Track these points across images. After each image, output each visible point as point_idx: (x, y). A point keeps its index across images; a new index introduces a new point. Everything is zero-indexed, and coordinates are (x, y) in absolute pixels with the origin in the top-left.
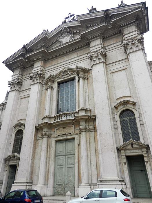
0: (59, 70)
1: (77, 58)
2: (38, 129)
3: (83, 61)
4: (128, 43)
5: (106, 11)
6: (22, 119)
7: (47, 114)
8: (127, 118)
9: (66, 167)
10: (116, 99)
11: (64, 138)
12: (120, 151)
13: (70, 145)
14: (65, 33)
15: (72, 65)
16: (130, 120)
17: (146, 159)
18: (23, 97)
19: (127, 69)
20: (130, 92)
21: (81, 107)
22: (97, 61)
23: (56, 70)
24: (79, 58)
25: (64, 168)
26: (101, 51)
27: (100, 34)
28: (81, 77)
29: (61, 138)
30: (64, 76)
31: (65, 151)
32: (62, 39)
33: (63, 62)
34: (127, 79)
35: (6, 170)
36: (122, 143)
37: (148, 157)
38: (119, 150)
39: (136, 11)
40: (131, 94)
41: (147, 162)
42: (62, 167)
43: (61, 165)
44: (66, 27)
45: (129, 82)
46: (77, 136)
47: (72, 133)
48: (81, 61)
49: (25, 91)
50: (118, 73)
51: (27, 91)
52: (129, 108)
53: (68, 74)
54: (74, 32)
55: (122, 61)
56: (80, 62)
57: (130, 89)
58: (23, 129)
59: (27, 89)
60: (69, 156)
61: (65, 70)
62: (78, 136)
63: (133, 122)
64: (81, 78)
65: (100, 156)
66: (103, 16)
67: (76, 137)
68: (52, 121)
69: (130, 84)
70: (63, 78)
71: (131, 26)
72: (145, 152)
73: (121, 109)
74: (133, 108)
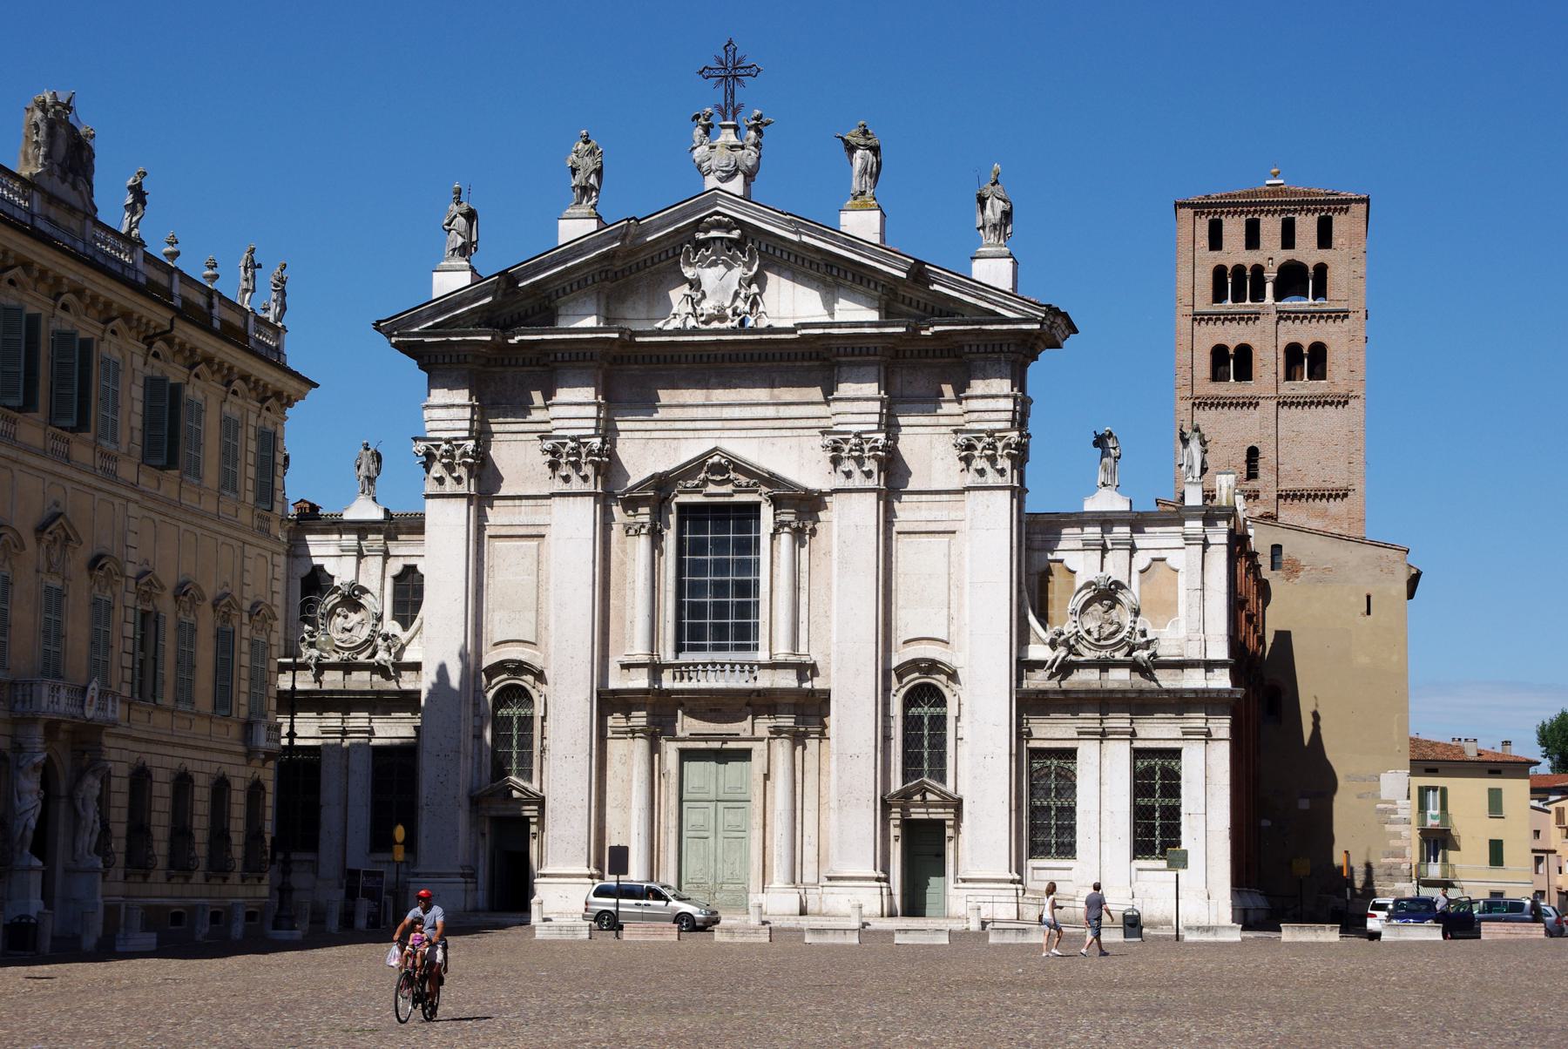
0: (689, 450)
1: (770, 412)
2: (609, 702)
3: (795, 432)
4: (975, 442)
5: (919, 263)
6: (512, 641)
7: (639, 652)
8: (925, 711)
9: (719, 836)
10: (900, 641)
11: (717, 745)
12: (891, 807)
13: (733, 767)
14: (718, 243)
15: (743, 433)
16: (932, 718)
17: (949, 832)
18: (503, 531)
19: (954, 532)
20: (949, 628)
21: (782, 651)
22: (858, 481)
23: (667, 434)
24: (781, 415)
25: (712, 839)
26: (876, 441)
27: (880, 349)
28: (788, 524)
29: (702, 745)
30: (711, 488)
31: (713, 787)
32: (699, 270)
33: (704, 405)
34: (947, 576)
35: (483, 835)
36: (897, 784)
37: (957, 827)
38: (886, 806)
39: (1024, 327)
40: (949, 633)
41: (950, 838)
42: (705, 834)
43: (702, 828)
44: (725, 215)
45: (952, 587)
46: (763, 745)
47: (743, 735)
48: (789, 433)
49: (510, 502)
50: (924, 539)
51: (517, 502)
52: (934, 682)
53: (728, 481)
54: (763, 248)
55: (945, 497)
56: (784, 432)
57: (949, 615)
58: (528, 687)
59: (520, 498)
60: (730, 804)
61: (716, 459)
62: (766, 747)
63: (939, 722)
64: (786, 529)
65: (833, 817)
66: (904, 275)
67: (758, 749)
68: (668, 682)
69: (952, 597)
70: (707, 495)
71: (999, 360)
72: (952, 816)
73: (914, 679)
74: (947, 687)
